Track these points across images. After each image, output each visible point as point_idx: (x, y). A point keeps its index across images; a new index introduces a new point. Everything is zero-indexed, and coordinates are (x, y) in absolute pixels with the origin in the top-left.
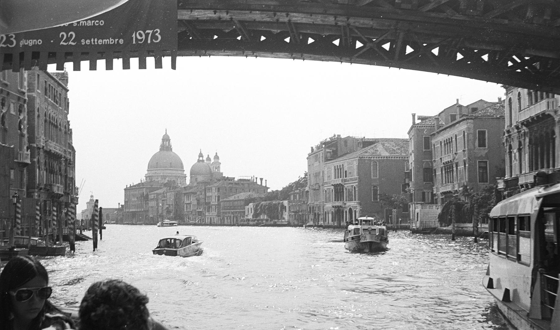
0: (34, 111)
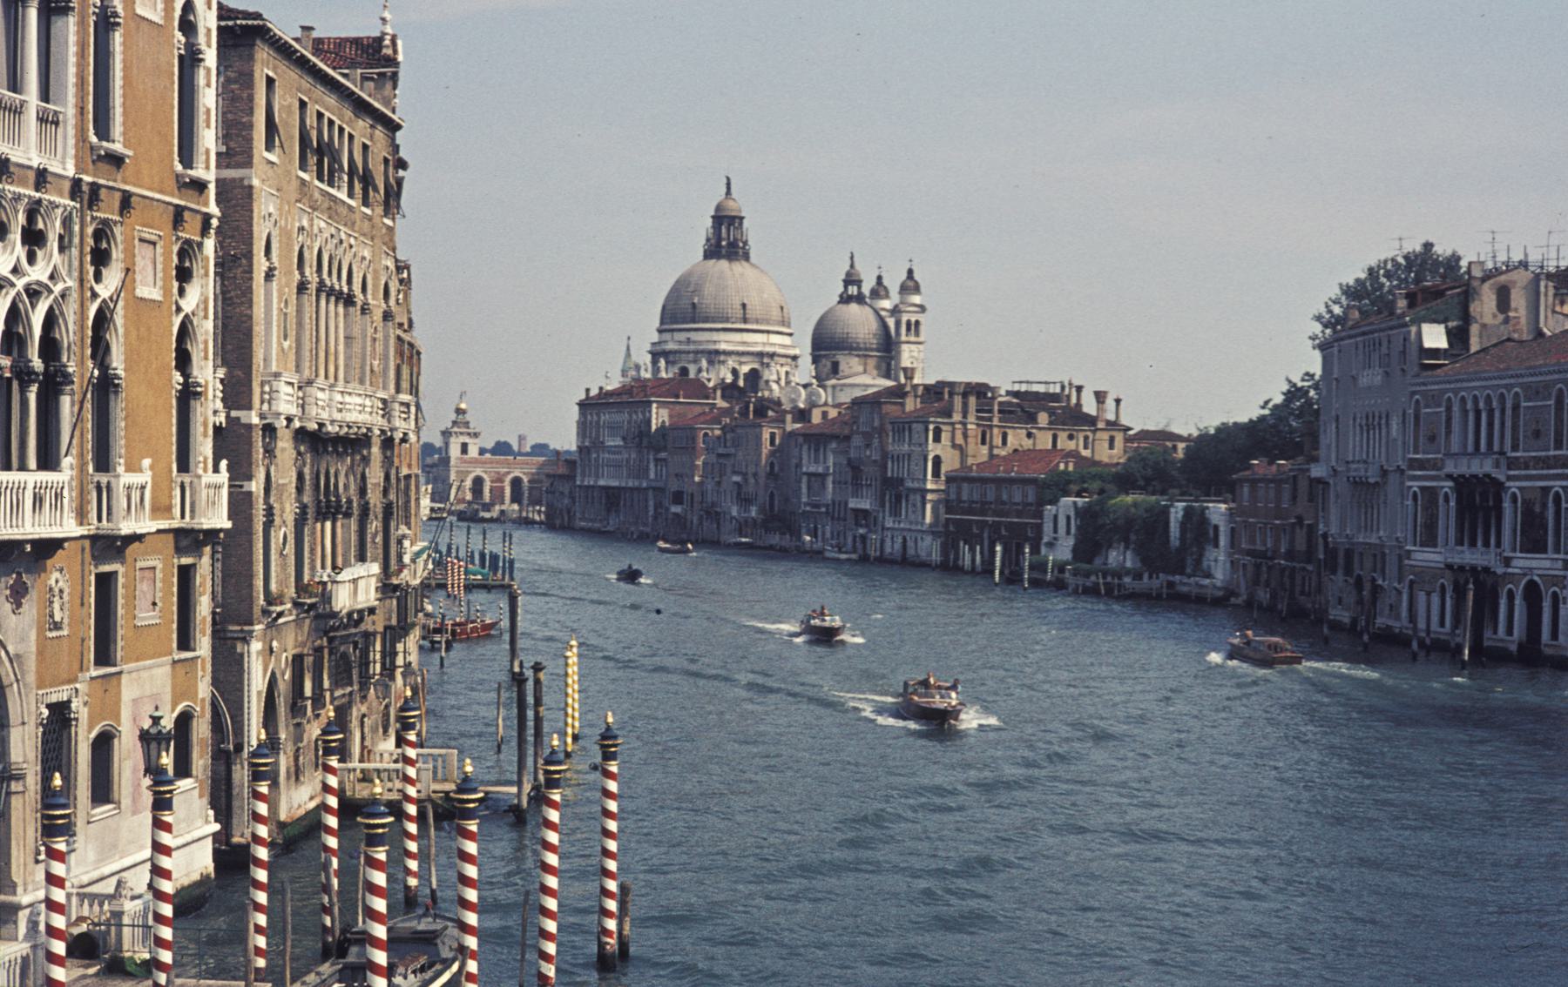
0: (249, 255)
